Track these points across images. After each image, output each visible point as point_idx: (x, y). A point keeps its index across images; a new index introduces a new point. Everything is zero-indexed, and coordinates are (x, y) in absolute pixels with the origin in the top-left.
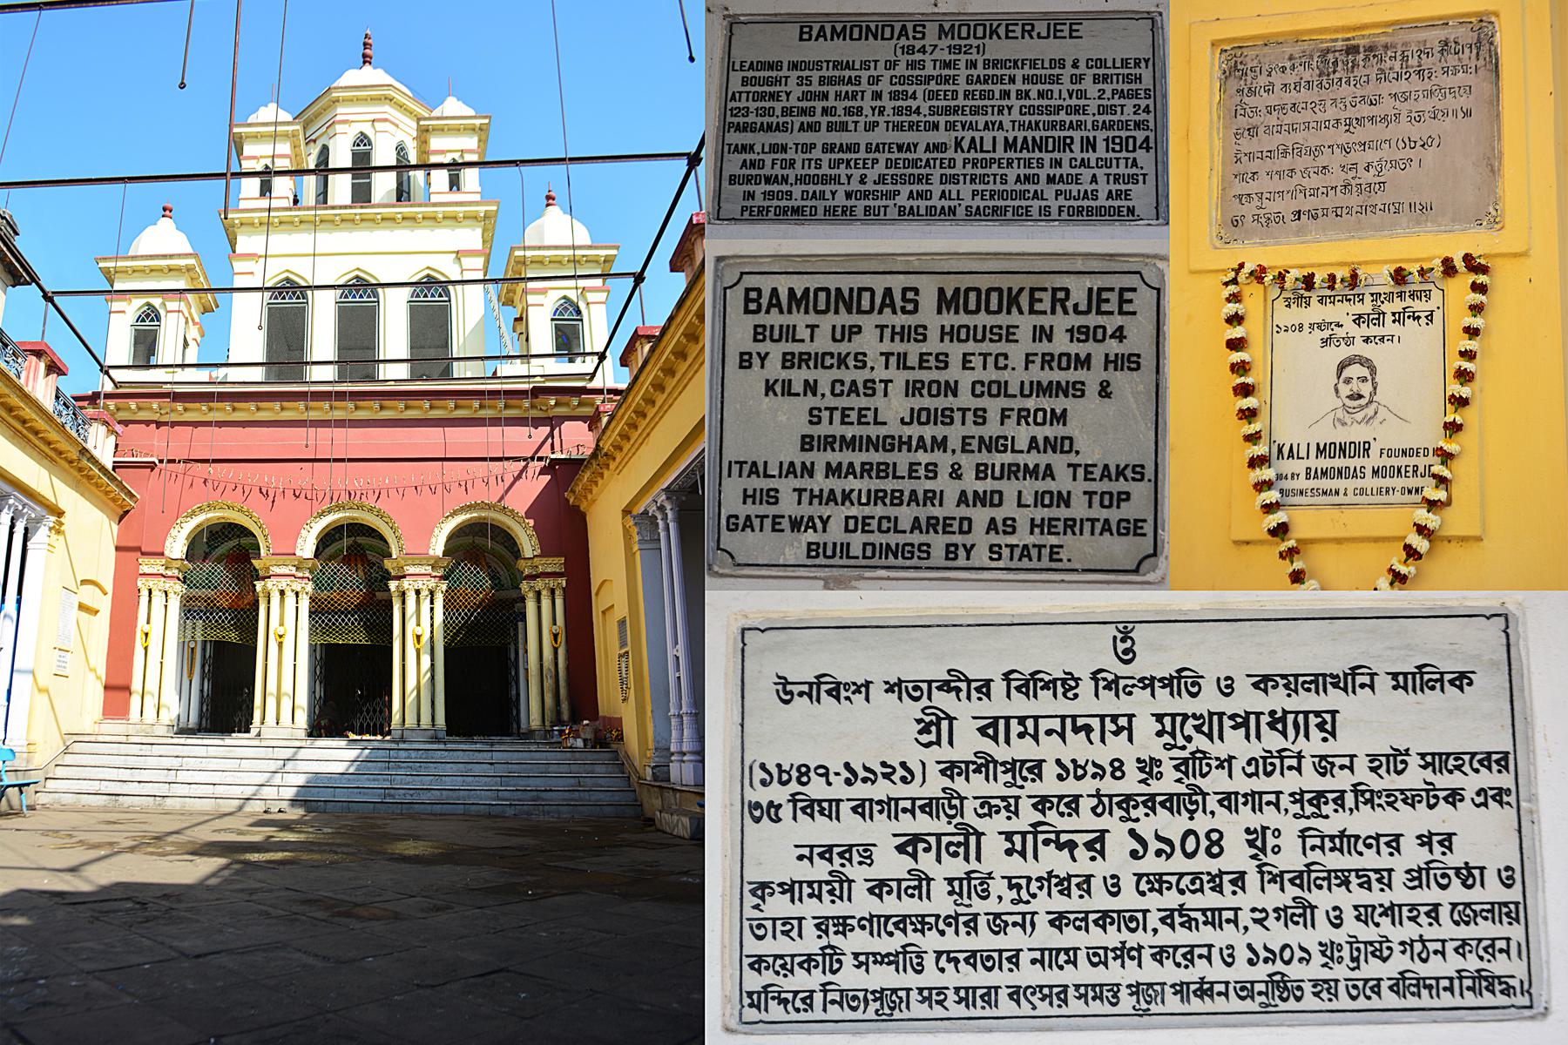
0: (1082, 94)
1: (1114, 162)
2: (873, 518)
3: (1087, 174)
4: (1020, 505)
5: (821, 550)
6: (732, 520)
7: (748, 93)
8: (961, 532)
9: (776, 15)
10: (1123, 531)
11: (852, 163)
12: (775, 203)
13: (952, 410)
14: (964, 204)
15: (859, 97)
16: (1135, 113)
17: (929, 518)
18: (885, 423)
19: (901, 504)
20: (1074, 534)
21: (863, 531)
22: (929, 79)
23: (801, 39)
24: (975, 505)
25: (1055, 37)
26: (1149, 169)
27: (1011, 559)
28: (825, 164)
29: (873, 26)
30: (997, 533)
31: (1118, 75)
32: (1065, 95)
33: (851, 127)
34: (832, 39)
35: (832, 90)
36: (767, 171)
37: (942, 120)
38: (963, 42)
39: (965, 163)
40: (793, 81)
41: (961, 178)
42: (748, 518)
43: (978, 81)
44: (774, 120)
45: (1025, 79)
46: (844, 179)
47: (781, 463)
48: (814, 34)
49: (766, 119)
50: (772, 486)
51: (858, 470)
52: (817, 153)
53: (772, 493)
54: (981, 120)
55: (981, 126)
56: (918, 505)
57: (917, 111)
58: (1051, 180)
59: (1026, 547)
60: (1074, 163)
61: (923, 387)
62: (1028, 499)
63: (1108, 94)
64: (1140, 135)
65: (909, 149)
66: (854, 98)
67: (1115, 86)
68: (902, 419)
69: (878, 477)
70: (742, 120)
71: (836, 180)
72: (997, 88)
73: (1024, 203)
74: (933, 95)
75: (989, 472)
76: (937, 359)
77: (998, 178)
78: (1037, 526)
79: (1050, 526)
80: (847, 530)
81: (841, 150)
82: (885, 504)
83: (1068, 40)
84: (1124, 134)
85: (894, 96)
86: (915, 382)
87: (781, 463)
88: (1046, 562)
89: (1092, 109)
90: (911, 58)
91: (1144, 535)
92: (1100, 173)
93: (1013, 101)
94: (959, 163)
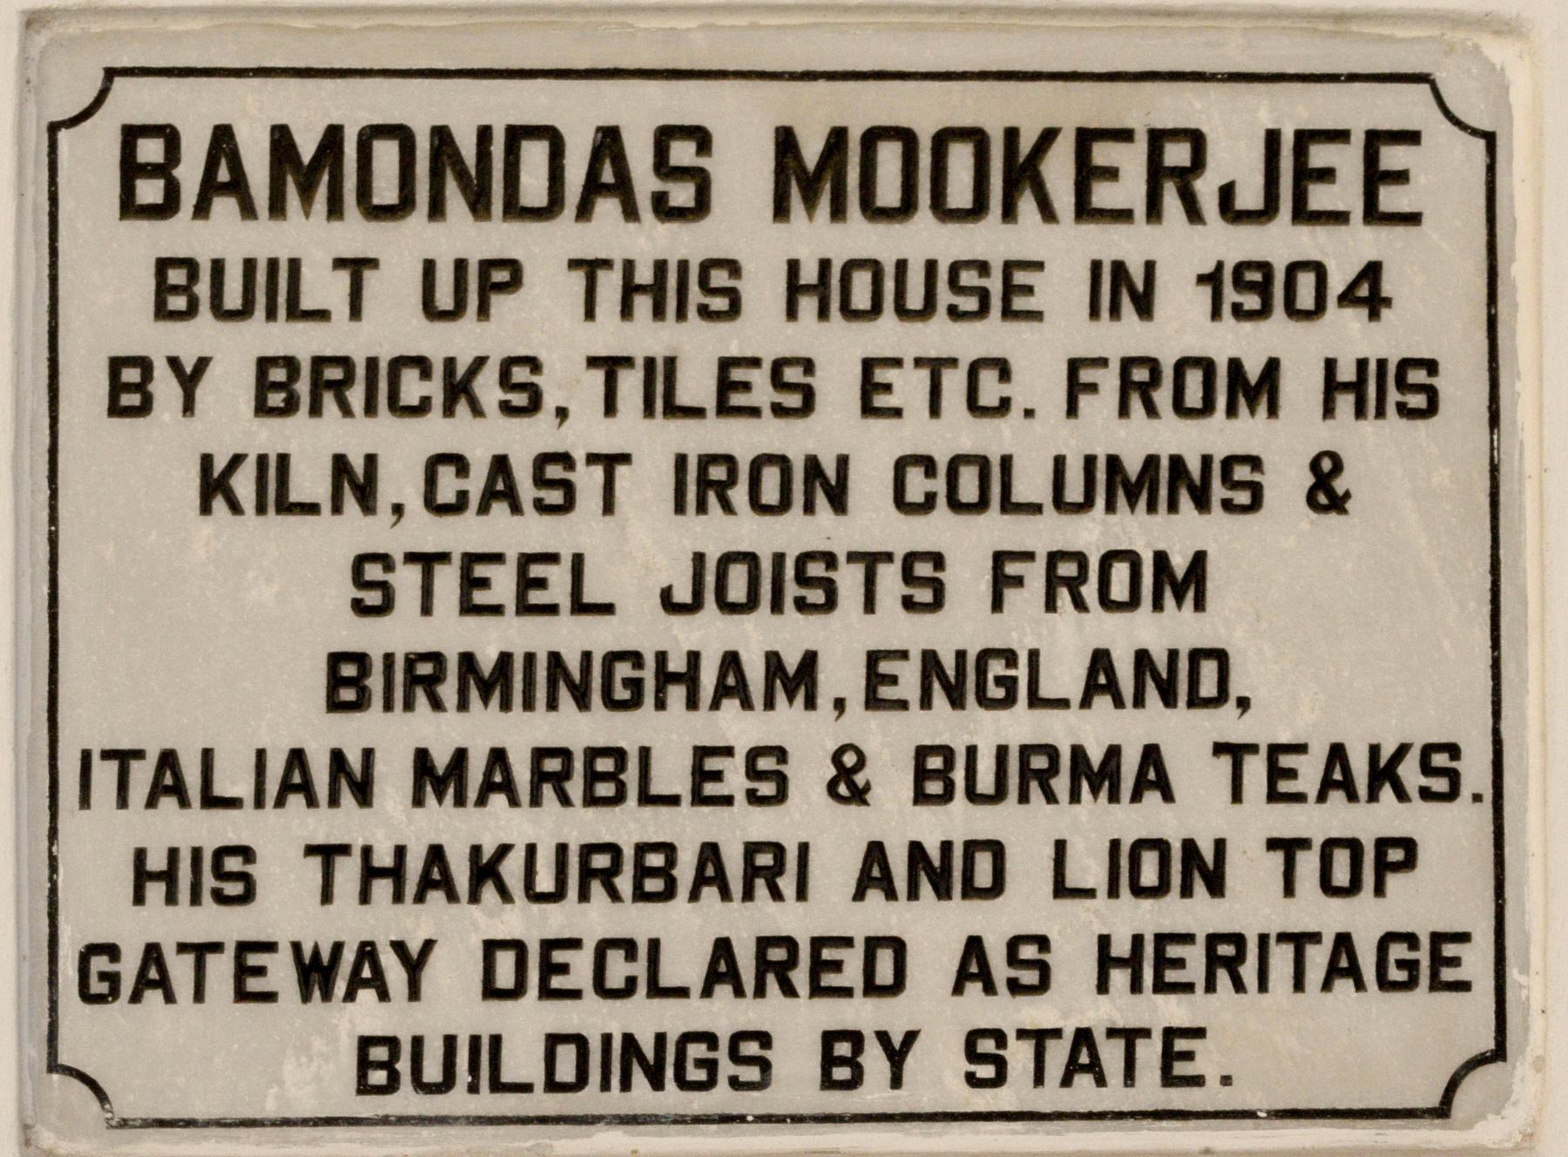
2: (574, 944)
4: (1061, 890)
5: (404, 1066)
6: (99, 963)
8: (872, 989)
10: (1396, 975)
13: (830, 560)
17: (764, 943)
18: (607, 609)
19: (669, 894)
20: (1239, 986)
21: (547, 993)
24: (913, 894)
27: (1039, 1079)
30: (989, 989)
42: (153, 953)
47: (261, 755)
50: (233, 840)
51: (522, 774)
53: (233, 864)
56: (725, 895)
59: (1084, 1037)
61: (732, 480)
62: (1088, 868)
68: (666, 595)
69: (591, 800)
75: (959, 775)
76: (778, 382)
78: (1120, 962)
79: (1162, 962)
80: (491, 991)
82: (615, 895)
86: (707, 461)
87: (261, 755)
88: (1149, 1091)
91: (1463, 986)
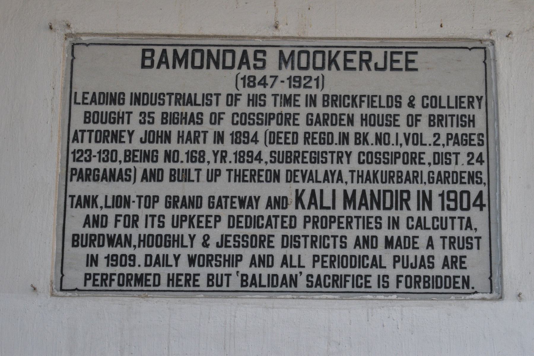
0: (418, 139)
1: (449, 221)
3: (423, 236)
7: (91, 131)
9: (118, 35)
11: (195, 221)
12: (118, 270)
14: (305, 272)
15: (201, 139)
16: (469, 163)
22: (270, 117)
23: (143, 66)
25: (392, 69)
26: (483, 232)
28: (168, 221)
29: (214, 50)
31: (452, 116)
32: (402, 140)
33: (194, 176)
34: (174, 67)
35: (174, 129)
36: (110, 230)
37: (283, 168)
38: (303, 73)
39: (305, 222)
40: (135, 118)
41: (302, 240)
43: (318, 122)
44: (116, 166)
45: (364, 120)
46: (187, 241)
48: (156, 59)
49: (109, 165)
52: (159, 209)
54: (321, 168)
55: (321, 177)
57: (259, 158)
58: (389, 243)
60: (411, 223)
63: (443, 140)
64: (474, 189)
65: (250, 205)
66: (196, 140)
67: (449, 130)
70: (84, 165)
71: (178, 241)
72: (336, 130)
73: (363, 272)
74: (274, 138)
77: (338, 240)
81: (184, 205)
83: (405, 74)
84: (458, 188)
85: (237, 138)
89: (428, 158)
90: (252, 91)
92: (436, 235)
93: (353, 148)
94: (300, 222)
